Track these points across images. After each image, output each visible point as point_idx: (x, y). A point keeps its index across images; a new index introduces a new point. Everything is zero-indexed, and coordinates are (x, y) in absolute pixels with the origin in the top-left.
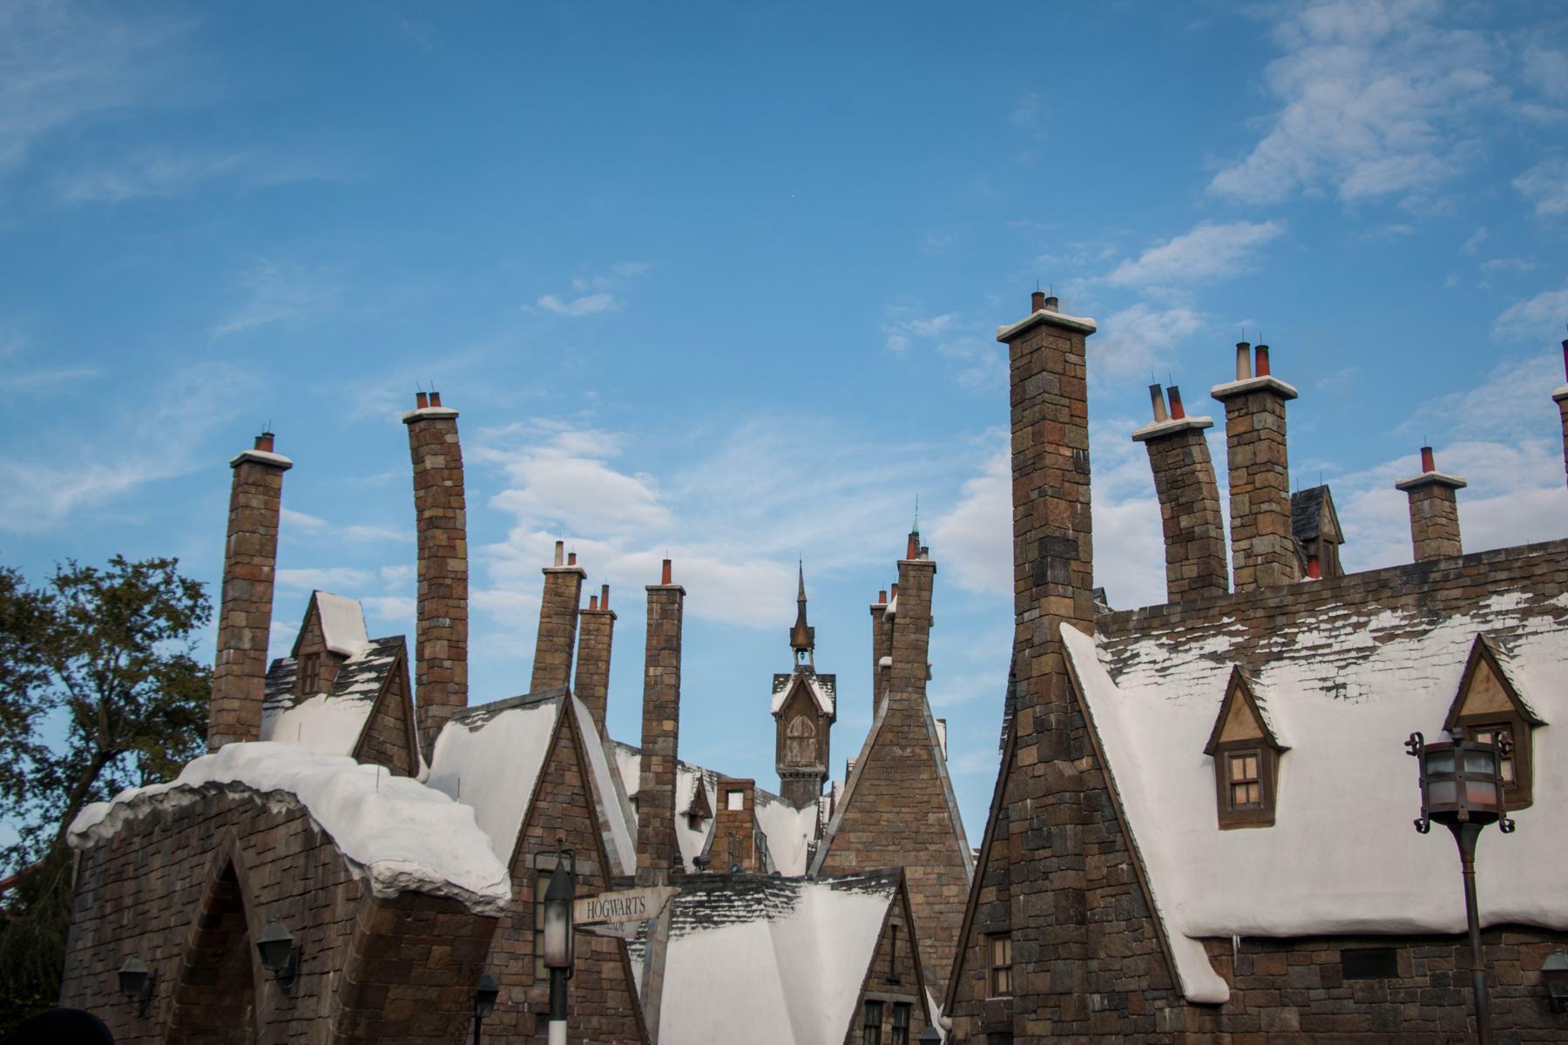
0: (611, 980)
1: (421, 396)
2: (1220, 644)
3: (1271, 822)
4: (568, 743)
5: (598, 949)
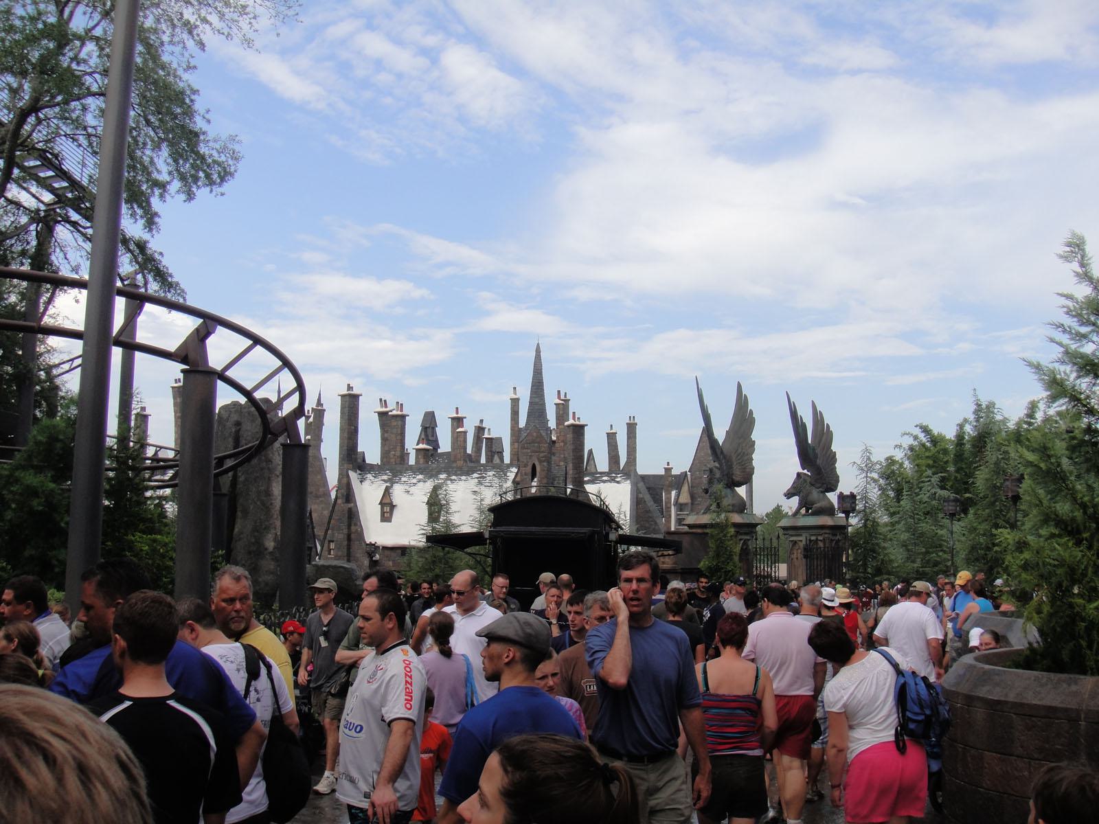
1: (176, 380)
2: (385, 477)
3: (390, 521)
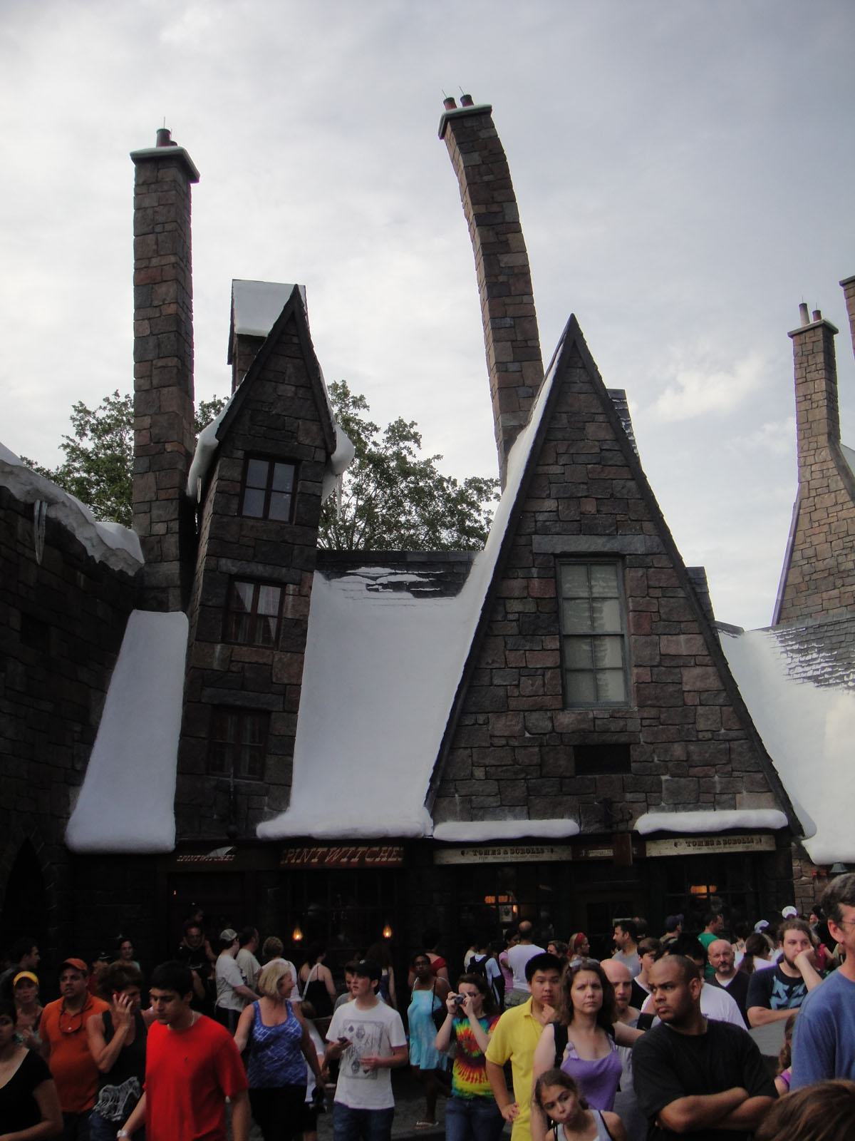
0: (699, 692)
4: (586, 387)
5: (673, 652)
